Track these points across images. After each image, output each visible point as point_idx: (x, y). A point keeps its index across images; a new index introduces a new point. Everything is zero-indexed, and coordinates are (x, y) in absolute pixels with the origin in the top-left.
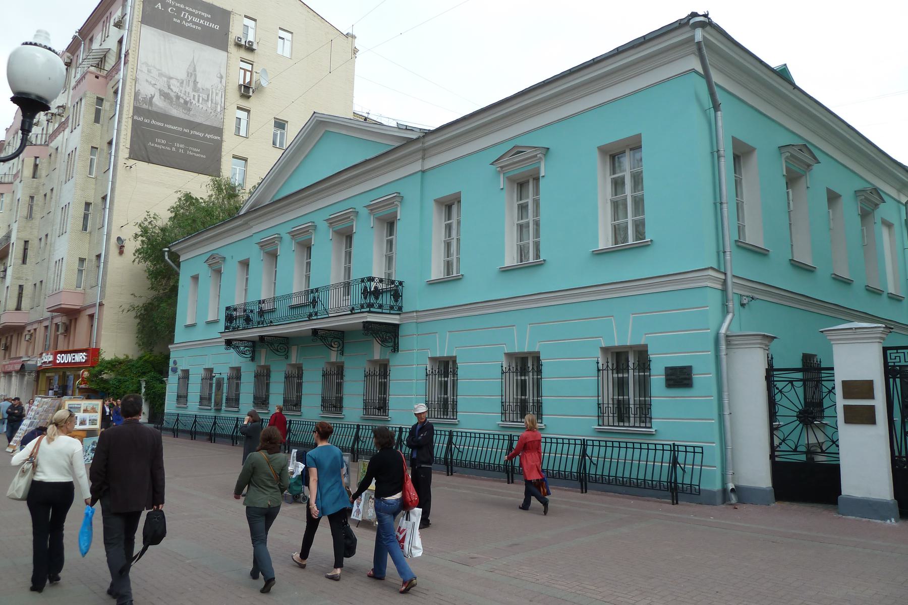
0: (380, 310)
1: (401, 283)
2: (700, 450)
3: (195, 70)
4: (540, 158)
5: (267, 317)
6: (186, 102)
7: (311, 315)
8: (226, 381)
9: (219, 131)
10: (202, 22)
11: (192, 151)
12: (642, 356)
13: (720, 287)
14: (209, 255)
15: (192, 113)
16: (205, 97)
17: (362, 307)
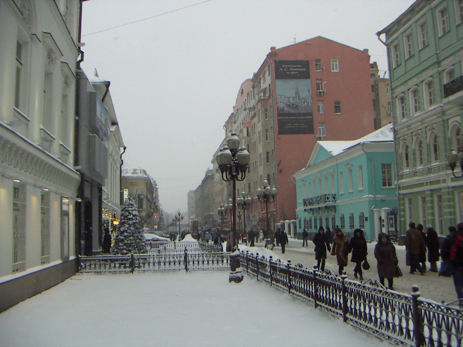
3: (298, 91)
6: (296, 106)
9: (311, 114)
10: (298, 69)
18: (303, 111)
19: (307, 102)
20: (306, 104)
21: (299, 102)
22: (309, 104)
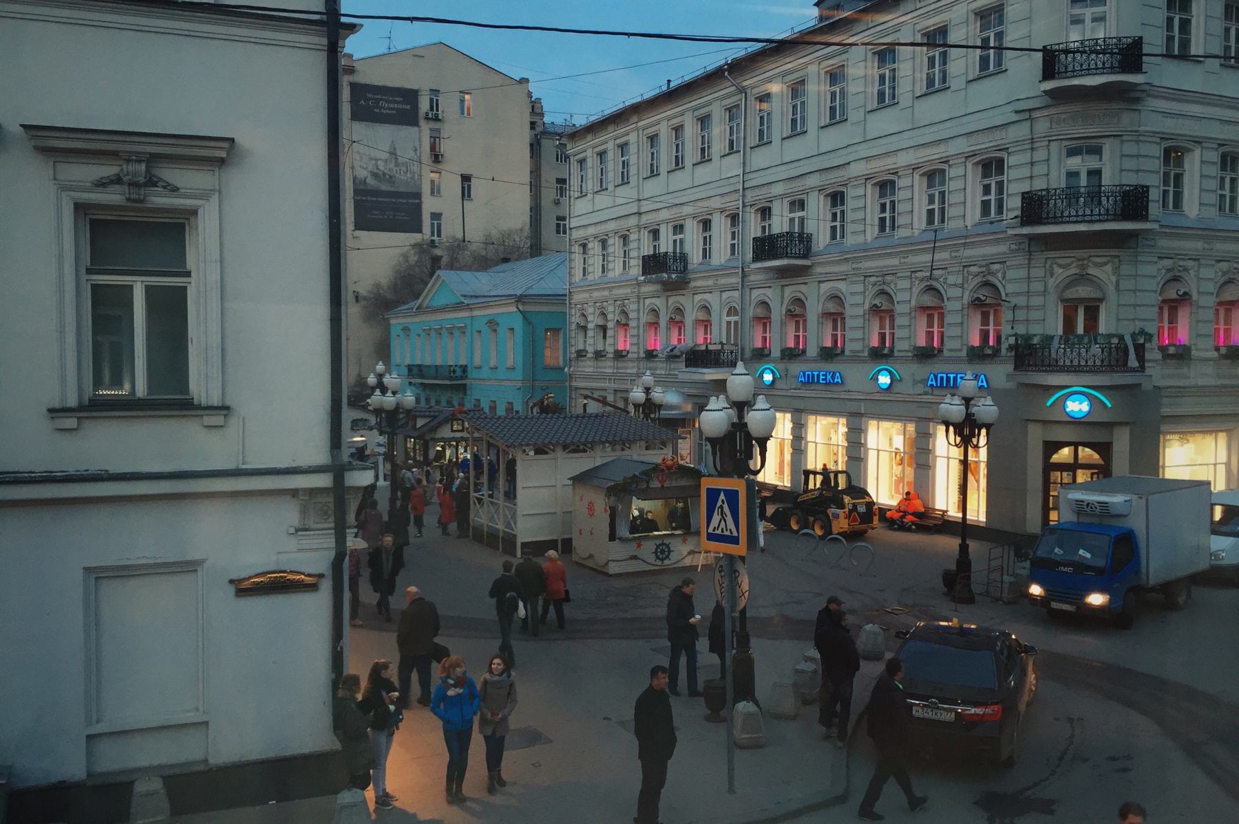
9: (418, 195)
18: (401, 190)
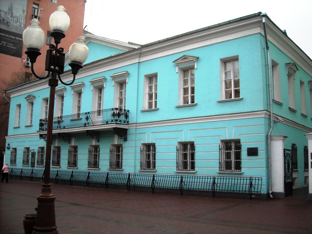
0: (120, 123)
1: (128, 111)
2: (261, 179)
4: (195, 61)
5: (62, 125)
6: (7, 22)
7: (85, 124)
8: (36, 153)
11: (9, 45)
12: (237, 143)
13: (268, 117)
14: (27, 95)
15: (10, 27)
16: (16, 20)
17: (112, 121)
19: (19, 23)
20: (18, 24)
21: (11, 19)
22: (21, 25)
